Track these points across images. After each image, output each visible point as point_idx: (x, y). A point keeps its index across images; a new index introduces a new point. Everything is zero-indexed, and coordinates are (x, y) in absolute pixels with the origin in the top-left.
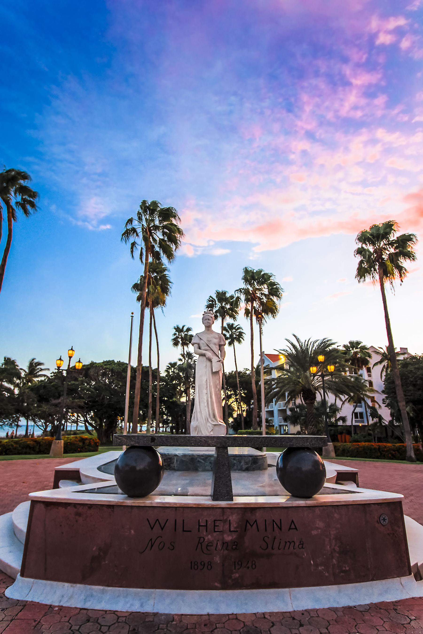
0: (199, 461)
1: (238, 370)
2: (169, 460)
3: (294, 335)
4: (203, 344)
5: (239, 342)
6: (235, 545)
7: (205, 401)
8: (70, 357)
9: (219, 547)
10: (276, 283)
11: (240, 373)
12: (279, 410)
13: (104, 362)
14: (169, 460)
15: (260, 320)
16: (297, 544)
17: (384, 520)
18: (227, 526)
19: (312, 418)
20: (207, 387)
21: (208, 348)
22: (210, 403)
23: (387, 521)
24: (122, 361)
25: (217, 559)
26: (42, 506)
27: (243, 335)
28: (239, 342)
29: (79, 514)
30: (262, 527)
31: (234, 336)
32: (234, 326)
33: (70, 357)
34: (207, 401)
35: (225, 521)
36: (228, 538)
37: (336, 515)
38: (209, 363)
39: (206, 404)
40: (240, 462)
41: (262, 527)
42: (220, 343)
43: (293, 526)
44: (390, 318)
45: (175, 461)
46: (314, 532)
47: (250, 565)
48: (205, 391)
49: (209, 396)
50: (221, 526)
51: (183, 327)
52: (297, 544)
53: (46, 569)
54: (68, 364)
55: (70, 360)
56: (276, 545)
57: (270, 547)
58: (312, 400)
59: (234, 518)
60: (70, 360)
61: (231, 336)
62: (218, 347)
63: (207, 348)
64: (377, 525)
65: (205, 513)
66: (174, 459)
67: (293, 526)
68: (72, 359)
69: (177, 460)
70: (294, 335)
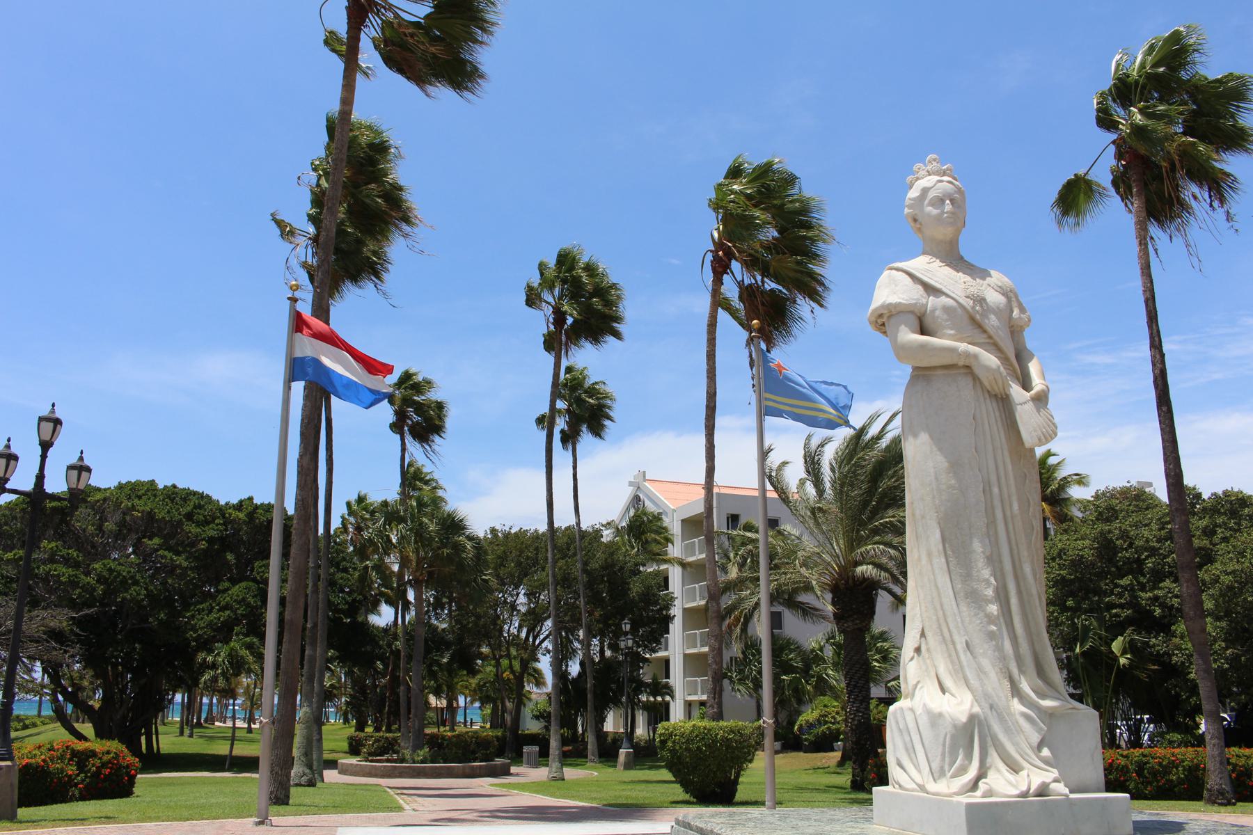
8: (46, 446)
11: (583, 534)
13: (121, 487)
20: (992, 523)
22: (1014, 601)
24: (181, 485)
33: (46, 446)
49: (1008, 567)
54: (37, 471)
55: (44, 457)
60: (44, 457)
68: (51, 452)
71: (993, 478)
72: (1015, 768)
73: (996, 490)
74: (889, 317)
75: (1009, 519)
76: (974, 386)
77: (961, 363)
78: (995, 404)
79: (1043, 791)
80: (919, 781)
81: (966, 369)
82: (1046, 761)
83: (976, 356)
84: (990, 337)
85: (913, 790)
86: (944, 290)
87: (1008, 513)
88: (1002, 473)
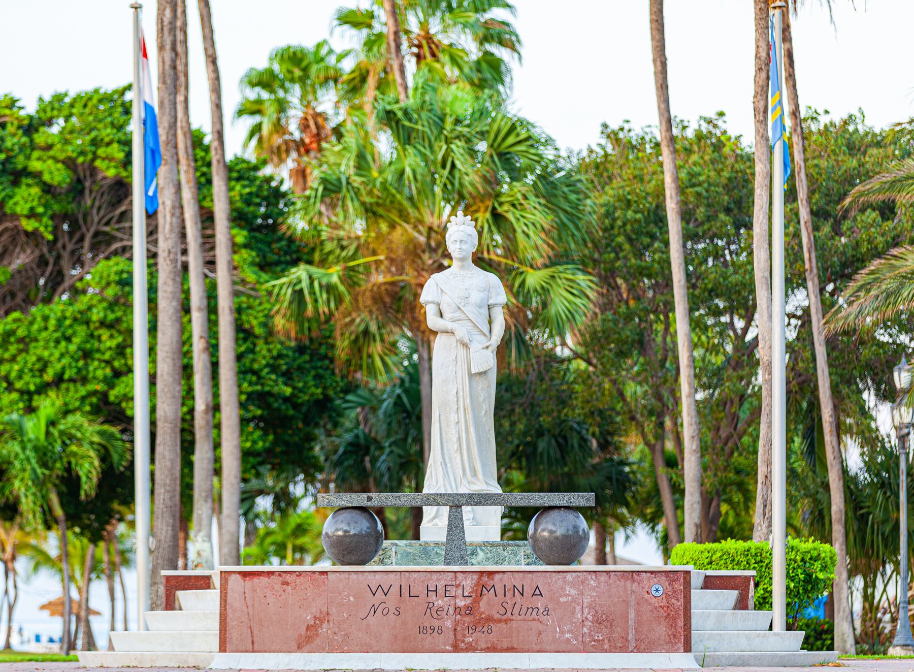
4: (449, 305)
6: (470, 610)
7: (455, 439)
9: (451, 611)
16: (541, 610)
17: (657, 590)
18: (460, 592)
23: (661, 592)
25: (449, 624)
26: (238, 577)
29: (287, 584)
30: (500, 592)
34: (459, 438)
35: (457, 586)
36: (461, 603)
37: (592, 582)
38: (462, 351)
39: (456, 446)
40: (516, 555)
41: (500, 592)
42: (491, 302)
43: (537, 592)
46: (562, 600)
47: (485, 629)
48: (453, 417)
50: (453, 591)
52: (541, 610)
53: (253, 643)
56: (516, 611)
57: (509, 613)
59: (468, 583)
62: (485, 311)
63: (458, 314)
64: (646, 596)
65: (435, 576)
67: (537, 592)
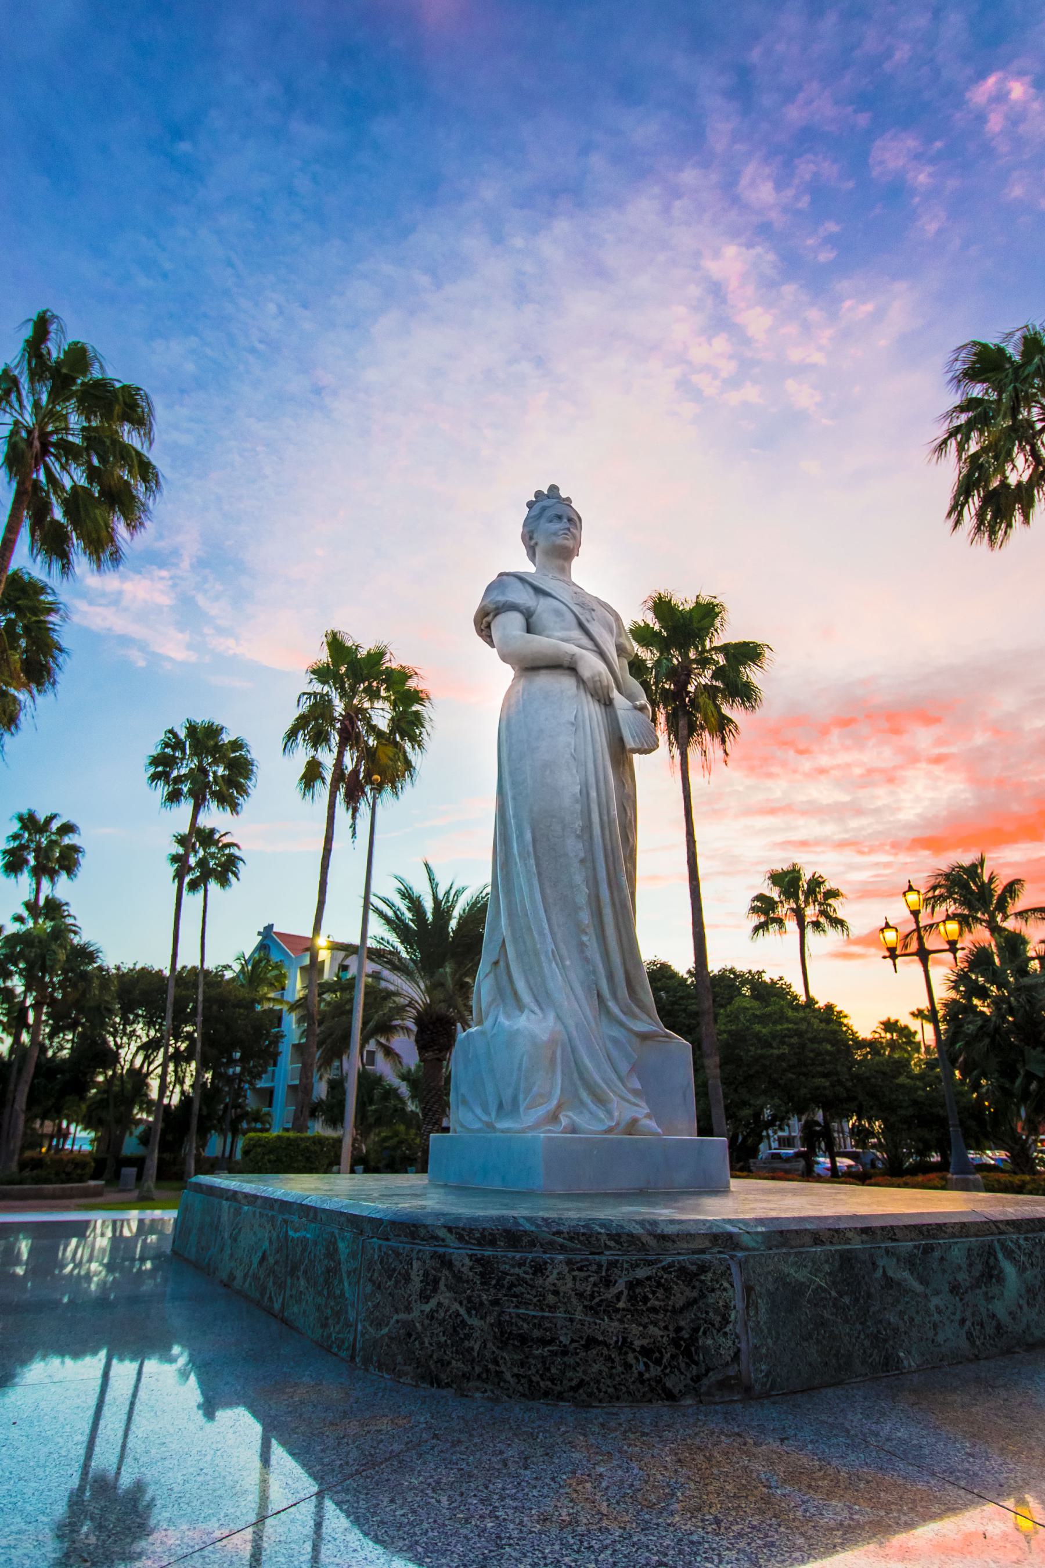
0: (889, 1283)
1: (206, 967)
2: (681, 1294)
3: (427, 865)
5: (224, 882)
7: (582, 898)
10: (425, 696)
11: (207, 973)
12: (290, 1087)
14: (681, 1294)
15: (353, 798)
19: (434, 1103)
21: (585, 641)
27: (240, 865)
28: (224, 882)
31: (212, 864)
32: (217, 836)
34: (595, 900)
44: (697, 838)
45: (739, 1302)
49: (602, 875)
51: (53, 817)
58: (440, 1051)
61: (202, 863)
63: (577, 634)
66: (727, 1273)
69: (748, 1290)
70: (427, 865)
71: (592, 780)
72: (600, 1100)
73: (593, 794)
74: (495, 616)
75: (606, 825)
76: (578, 687)
77: (566, 664)
78: (597, 708)
79: (632, 1126)
80: (485, 1118)
81: (569, 667)
82: (635, 1092)
83: (582, 657)
84: (597, 645)
85: (479, 1130)
86: (554, 593)
87: (605, 818)
88: (601, 778)
